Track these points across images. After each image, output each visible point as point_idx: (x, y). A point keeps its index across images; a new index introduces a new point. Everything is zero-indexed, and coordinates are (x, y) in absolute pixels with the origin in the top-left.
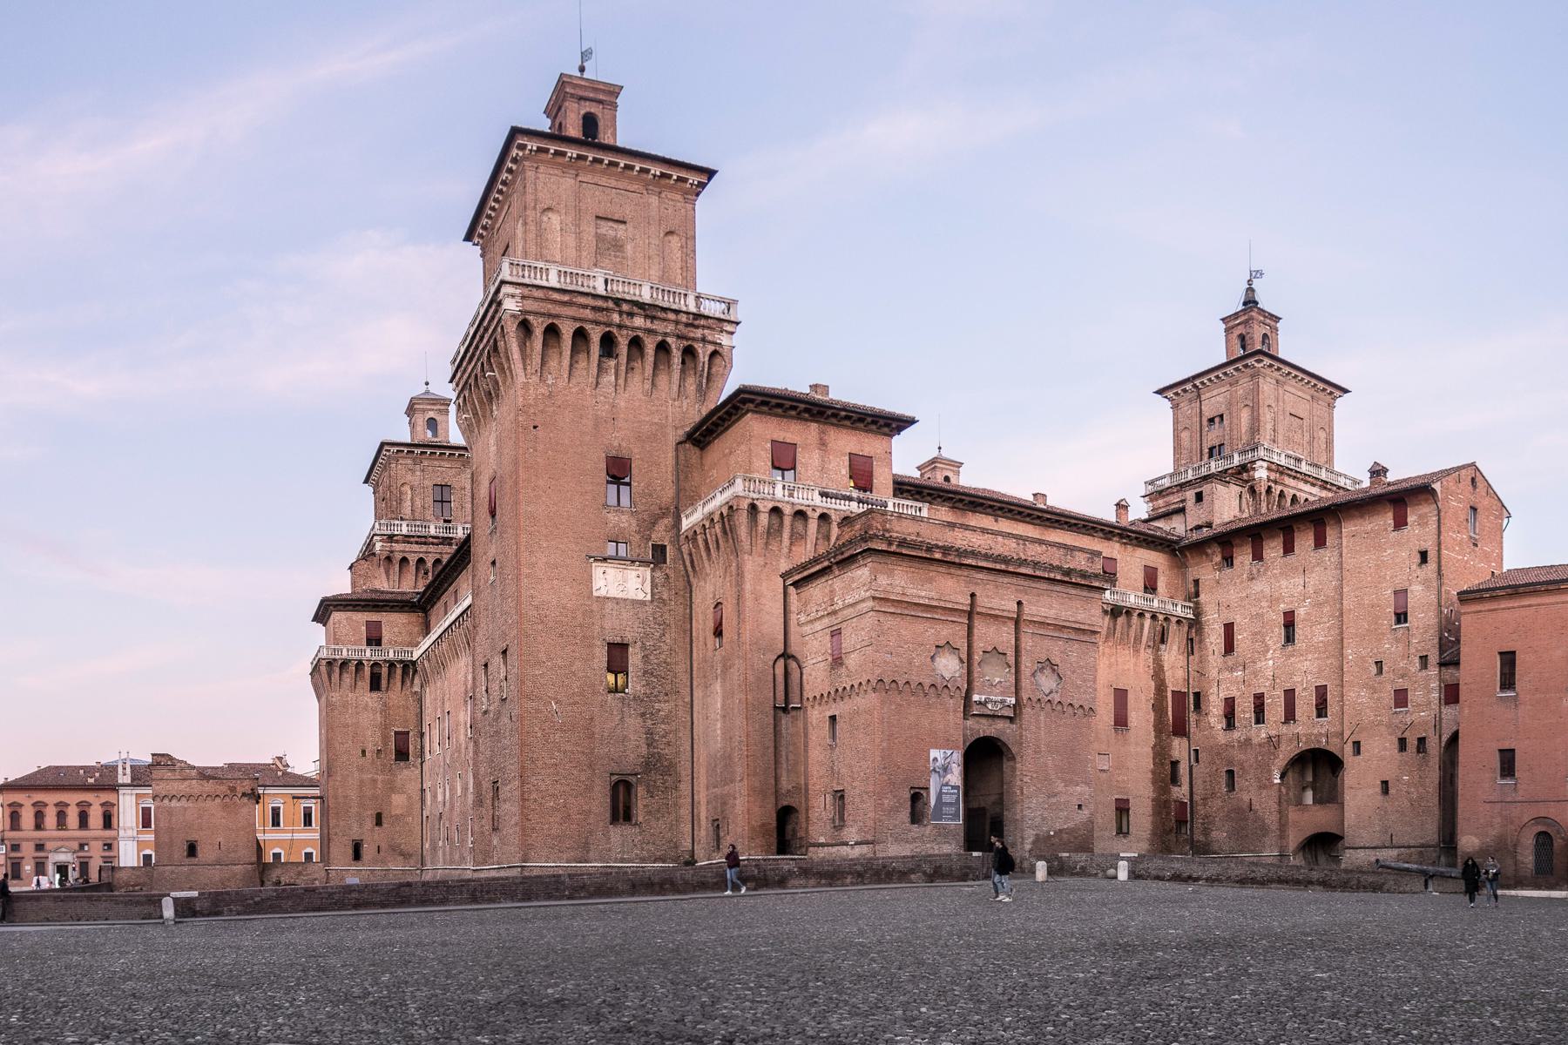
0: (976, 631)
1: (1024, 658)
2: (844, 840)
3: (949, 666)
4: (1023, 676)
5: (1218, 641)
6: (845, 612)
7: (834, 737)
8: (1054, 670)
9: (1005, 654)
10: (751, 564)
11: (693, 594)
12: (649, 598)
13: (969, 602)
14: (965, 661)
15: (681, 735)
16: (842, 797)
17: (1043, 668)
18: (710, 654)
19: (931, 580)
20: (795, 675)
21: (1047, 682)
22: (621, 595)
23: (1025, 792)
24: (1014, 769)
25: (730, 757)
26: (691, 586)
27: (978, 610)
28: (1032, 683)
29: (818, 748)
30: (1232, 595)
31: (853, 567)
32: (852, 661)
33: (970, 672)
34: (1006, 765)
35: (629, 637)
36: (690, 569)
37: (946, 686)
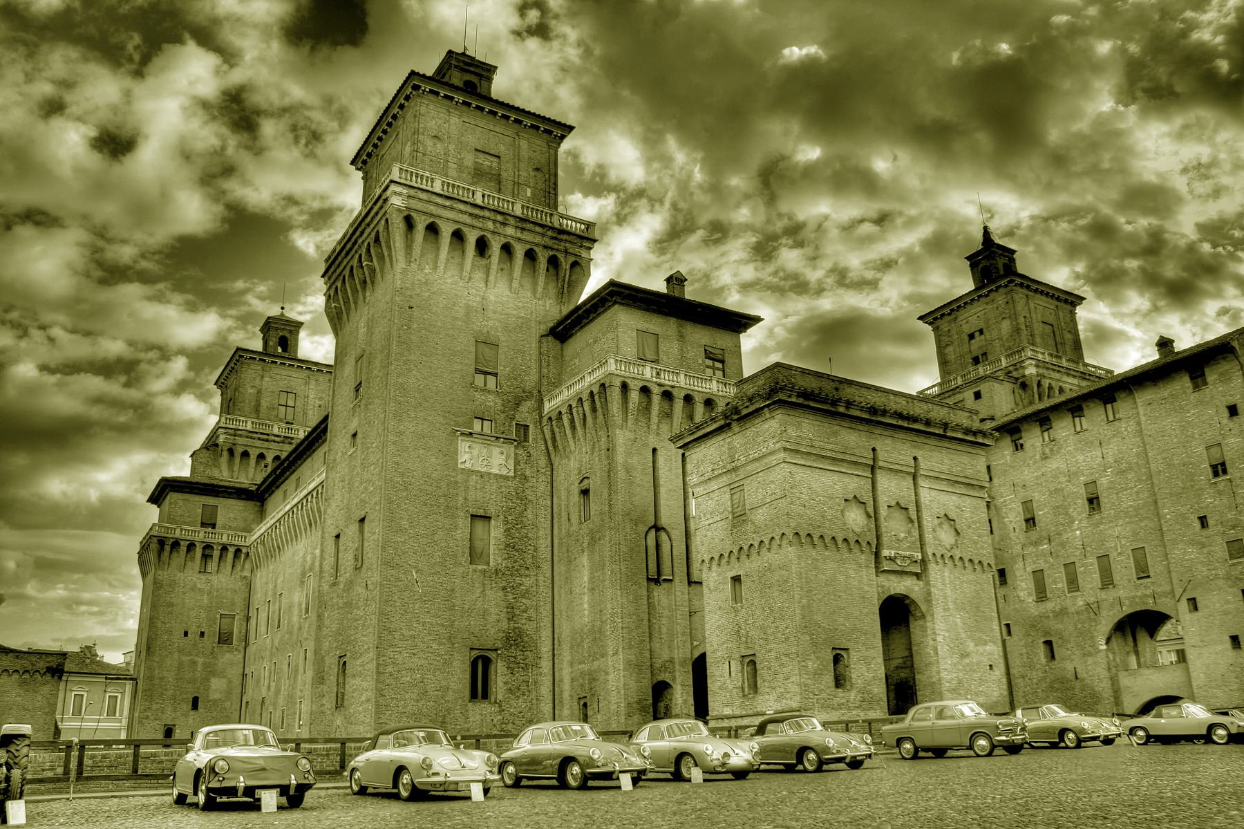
1: (924, 513)
2: (759, 710)
3: (855, 518)
4: (926, 531)
5: (1018, 519)
6: (748, 468)
7: (736, 597)
8: (951, 525)
9: (907, 509)
10: (622, 437)
12: (512, 474)
13: (872, 456)
14: (873, 515)
15: (541, 610)
16: (753, 663)
17: (940, 524)
18: (574, 528)
19: (835, 434)
20: (666, 548)
22: (484, 470)
23: (939, 653)
24: (924, 629)
25: (600, 631)
26: (552, 465)
27: (881, 464)
28: (934, 537)
29: (718, 612)
30: (1027, 475)
31: (757, 421)
32: (760, 516)
33: (877, 527)
34: (915, 626)
35: (492, 511)
36: (551, 448)
37: (857, 541)
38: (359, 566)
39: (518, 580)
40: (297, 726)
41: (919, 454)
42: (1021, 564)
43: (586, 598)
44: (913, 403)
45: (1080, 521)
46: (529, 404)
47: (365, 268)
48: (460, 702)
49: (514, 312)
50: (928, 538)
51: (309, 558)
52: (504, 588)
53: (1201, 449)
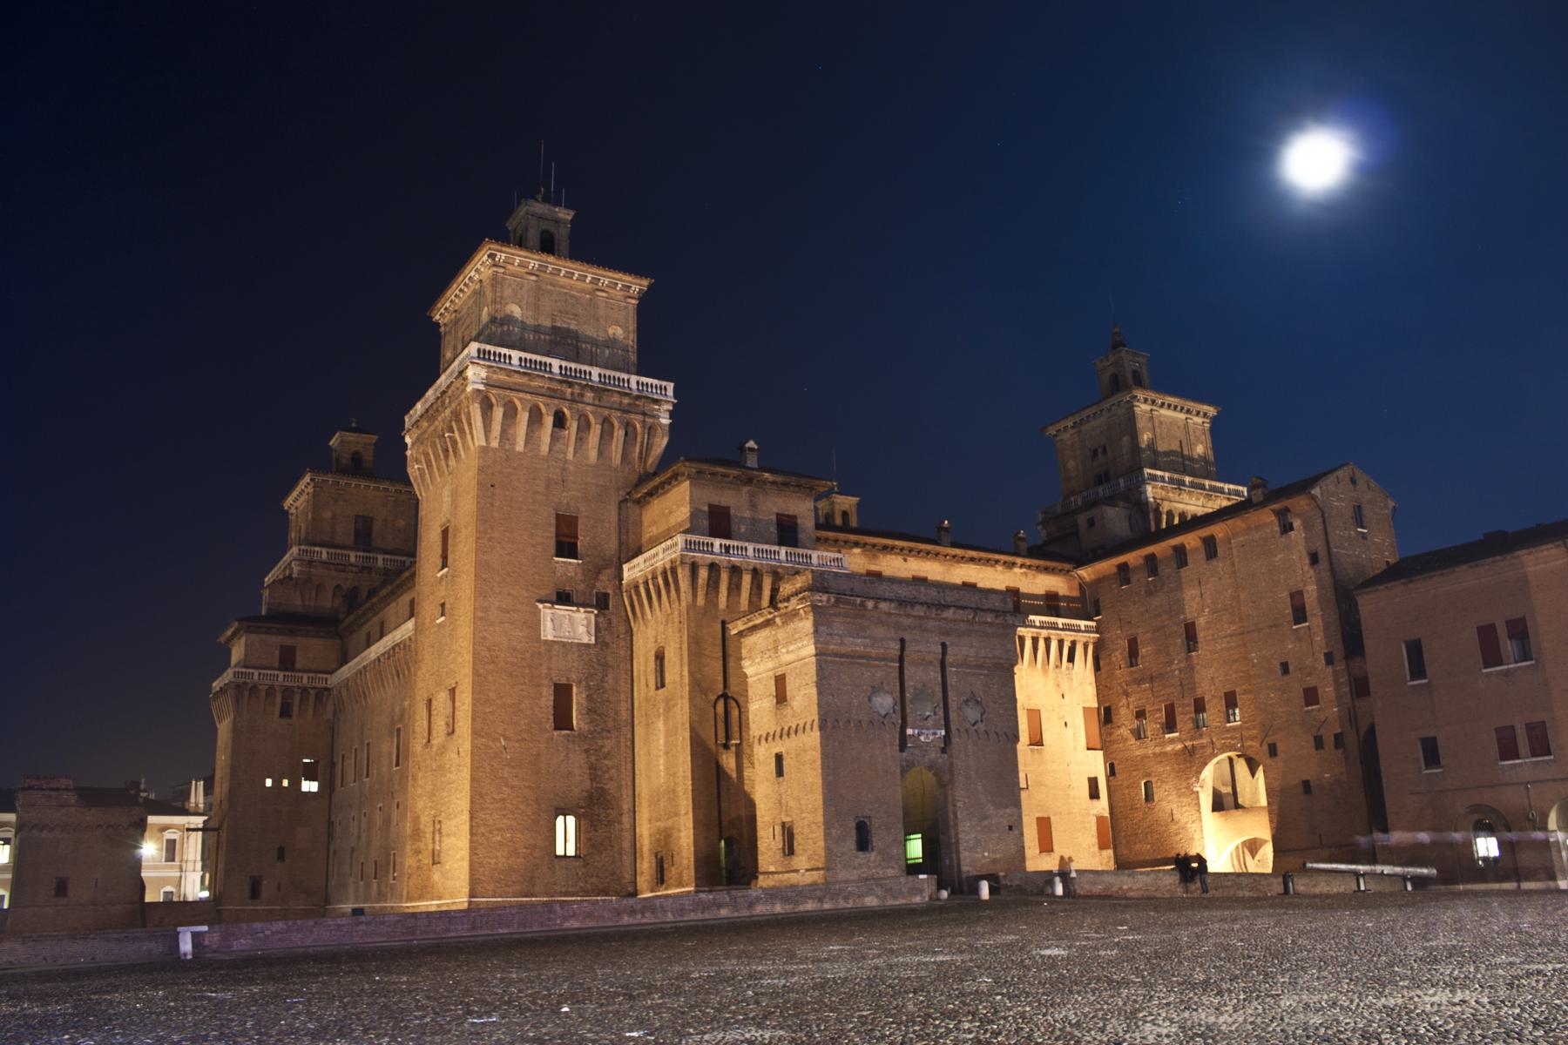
0: (906, 671)
3: (885, 702)
11: (634, 638)
12: (593, 641)
20: (735, 713)
21: (973, 714)
25: (674, 791)
38: (450, 730)
39: (600, 743)
40: (391, 878)
41: (948, 641)
42: (1124, 701)
43: (662, 761)
44: (944, 592)
45: (1180, 662)
46: (609, 571)
47: (448, 440)
48: (547, 858)
49: (594, 481)
50: (953, 715)
51: (397, 709)
52: (587, 751)
53: (1285, 594)
